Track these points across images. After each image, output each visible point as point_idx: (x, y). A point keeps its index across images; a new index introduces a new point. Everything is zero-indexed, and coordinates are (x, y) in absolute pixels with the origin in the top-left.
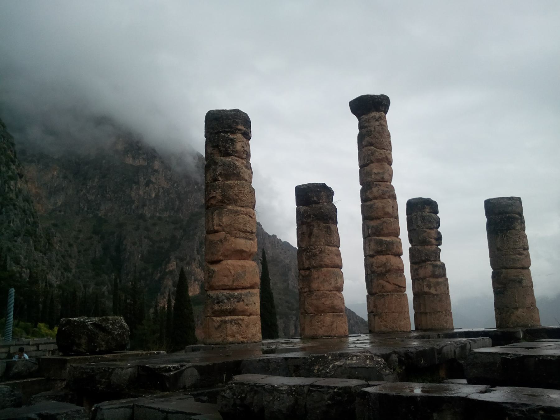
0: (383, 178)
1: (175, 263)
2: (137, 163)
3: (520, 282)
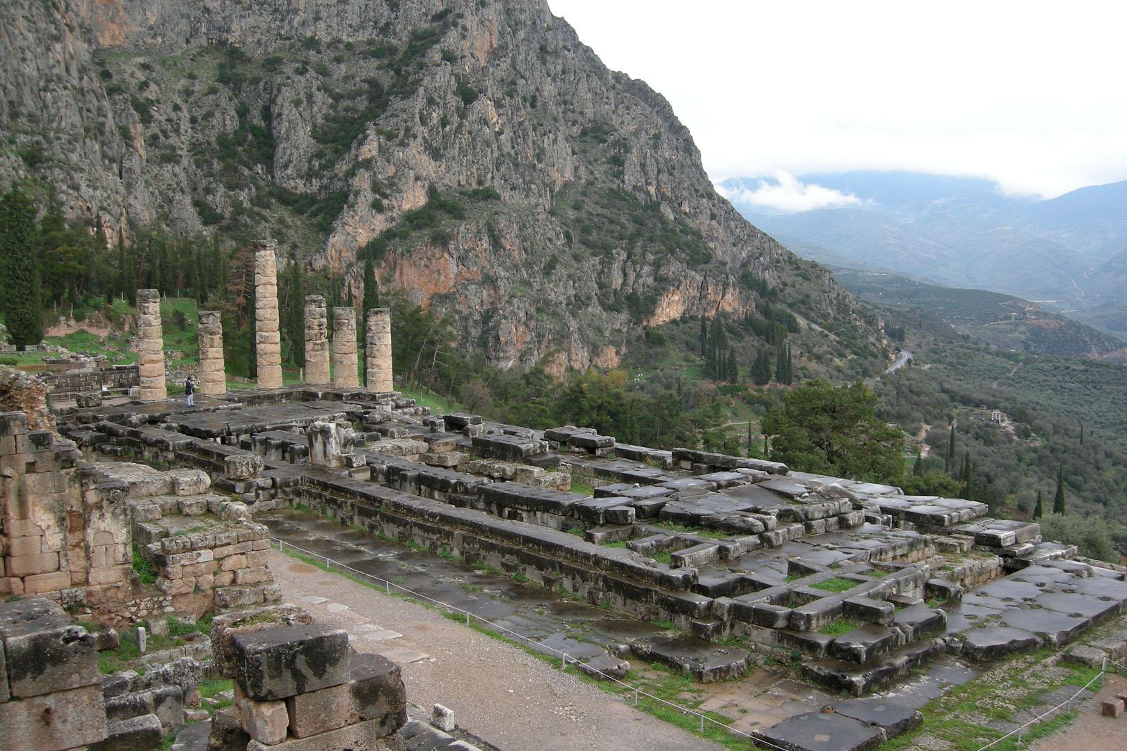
1: (376, 144)
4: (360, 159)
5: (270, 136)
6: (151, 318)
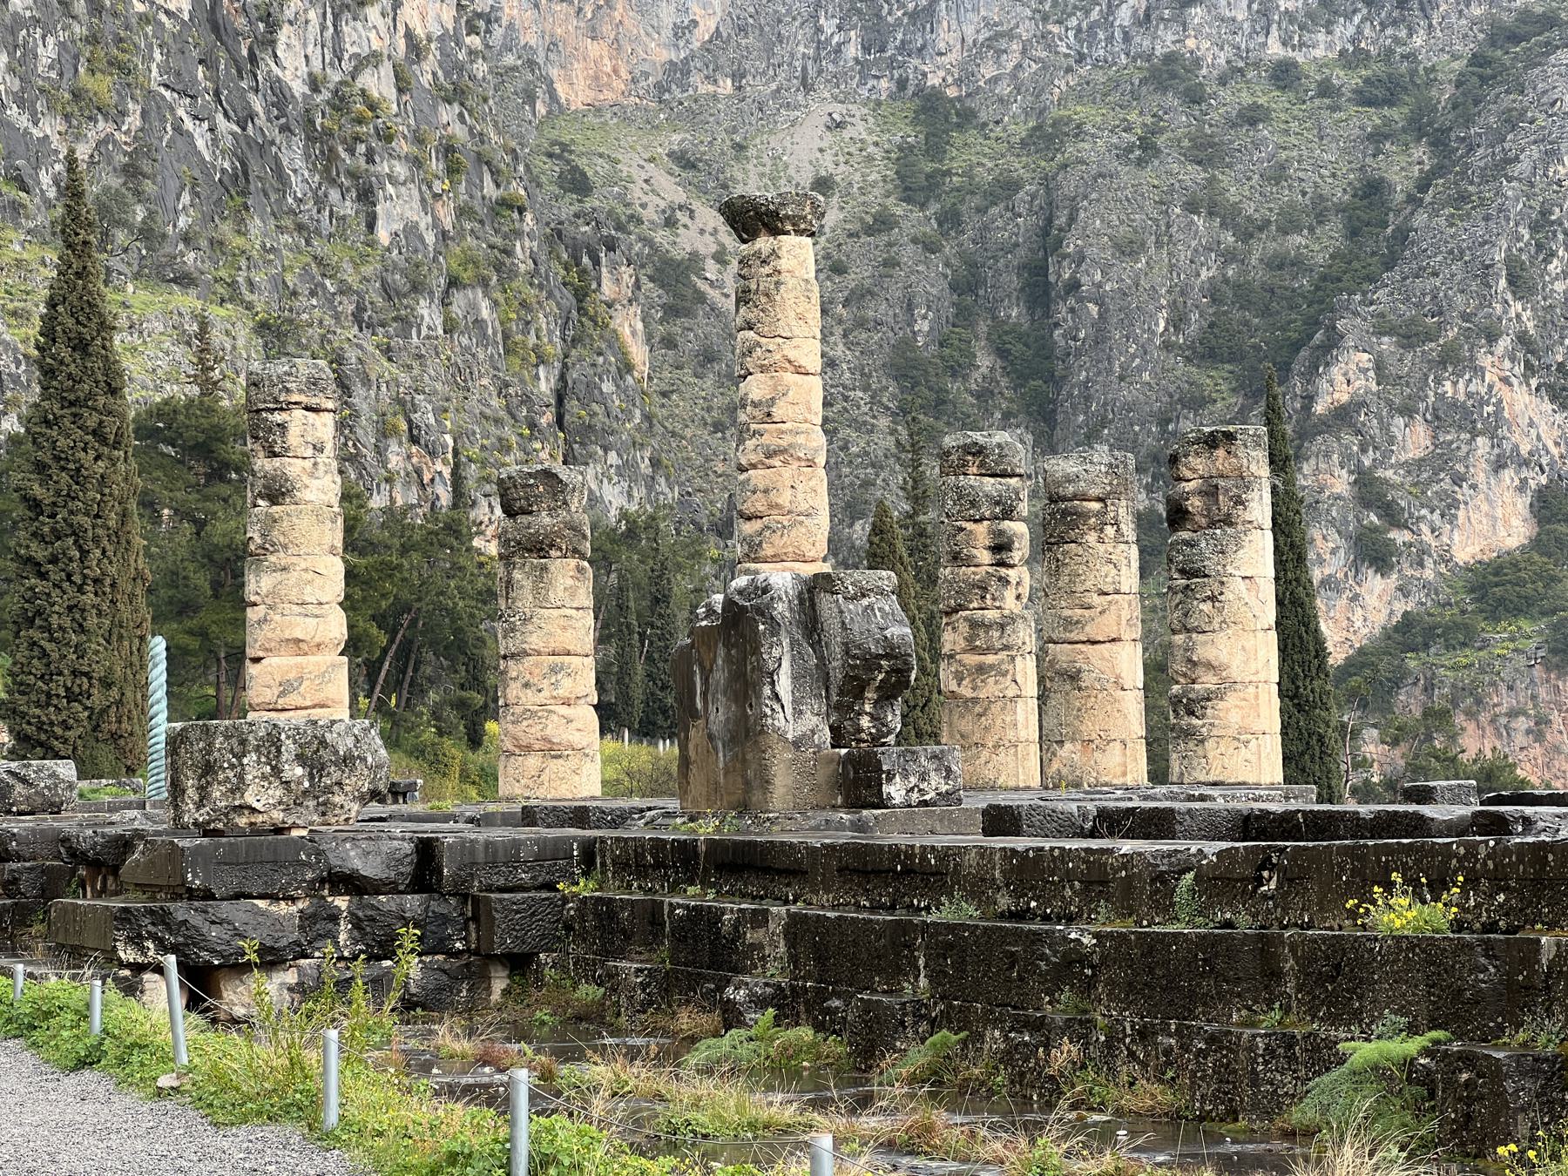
0: (769, 415)
3: (1074, 677)
4: (1319, 408)
5: (1045, 350)
6: (294, 468)
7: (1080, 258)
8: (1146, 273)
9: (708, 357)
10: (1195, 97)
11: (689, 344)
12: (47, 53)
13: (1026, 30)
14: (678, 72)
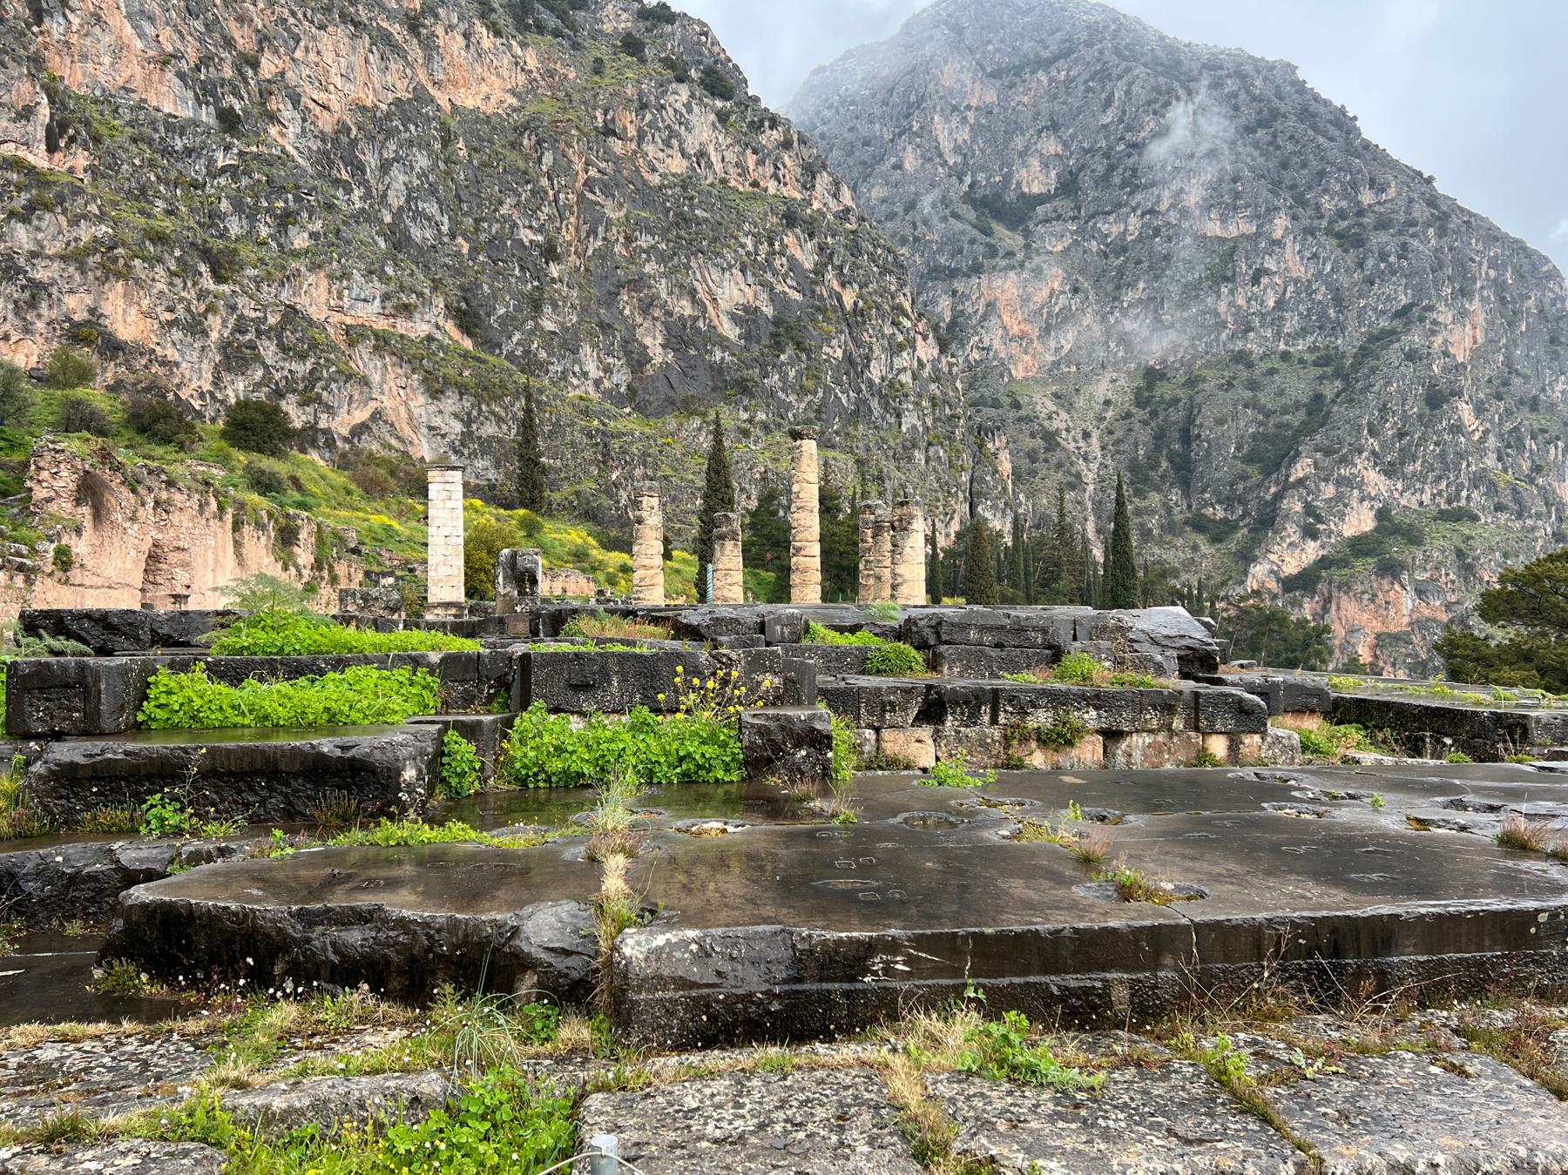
2: (1233, 231)
5: (1188, 460)
7: (1201, 426)
8: (1227, 432)
9: (1060, 465)
10: (1250, 366)
11: (1054, 461)
12: (792, 374)
13: (1186, 344)
14: (1056, 364)
